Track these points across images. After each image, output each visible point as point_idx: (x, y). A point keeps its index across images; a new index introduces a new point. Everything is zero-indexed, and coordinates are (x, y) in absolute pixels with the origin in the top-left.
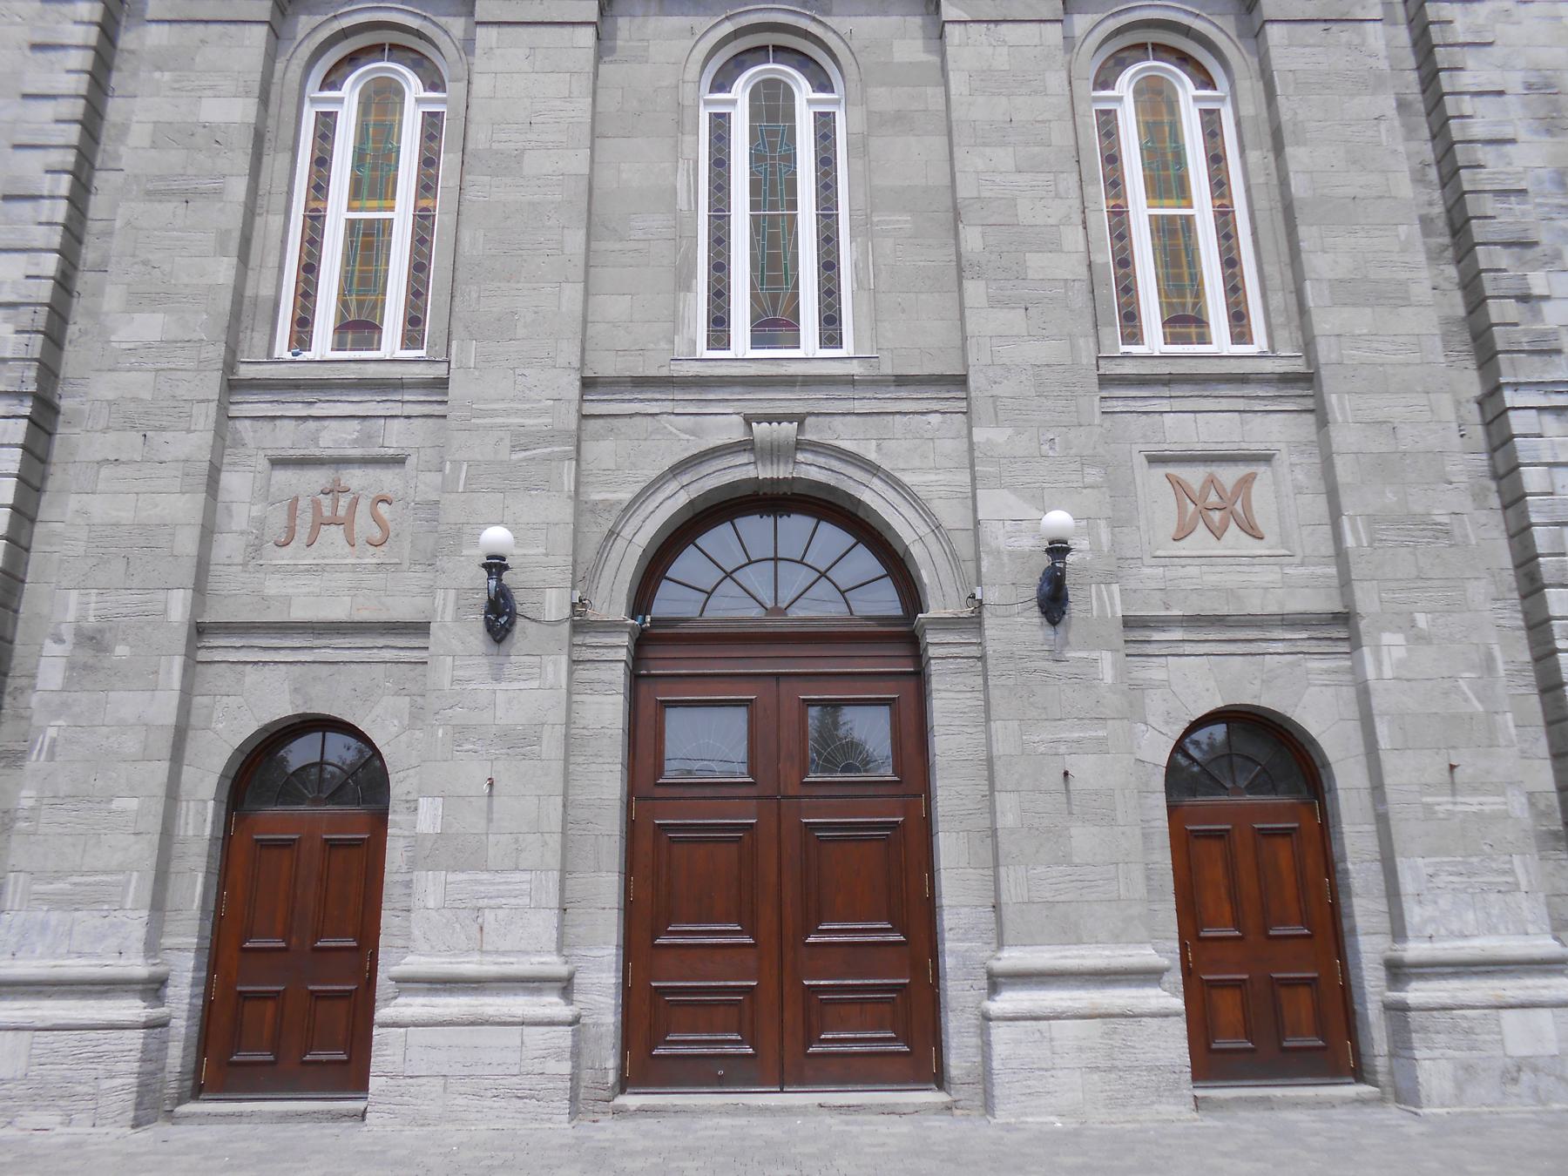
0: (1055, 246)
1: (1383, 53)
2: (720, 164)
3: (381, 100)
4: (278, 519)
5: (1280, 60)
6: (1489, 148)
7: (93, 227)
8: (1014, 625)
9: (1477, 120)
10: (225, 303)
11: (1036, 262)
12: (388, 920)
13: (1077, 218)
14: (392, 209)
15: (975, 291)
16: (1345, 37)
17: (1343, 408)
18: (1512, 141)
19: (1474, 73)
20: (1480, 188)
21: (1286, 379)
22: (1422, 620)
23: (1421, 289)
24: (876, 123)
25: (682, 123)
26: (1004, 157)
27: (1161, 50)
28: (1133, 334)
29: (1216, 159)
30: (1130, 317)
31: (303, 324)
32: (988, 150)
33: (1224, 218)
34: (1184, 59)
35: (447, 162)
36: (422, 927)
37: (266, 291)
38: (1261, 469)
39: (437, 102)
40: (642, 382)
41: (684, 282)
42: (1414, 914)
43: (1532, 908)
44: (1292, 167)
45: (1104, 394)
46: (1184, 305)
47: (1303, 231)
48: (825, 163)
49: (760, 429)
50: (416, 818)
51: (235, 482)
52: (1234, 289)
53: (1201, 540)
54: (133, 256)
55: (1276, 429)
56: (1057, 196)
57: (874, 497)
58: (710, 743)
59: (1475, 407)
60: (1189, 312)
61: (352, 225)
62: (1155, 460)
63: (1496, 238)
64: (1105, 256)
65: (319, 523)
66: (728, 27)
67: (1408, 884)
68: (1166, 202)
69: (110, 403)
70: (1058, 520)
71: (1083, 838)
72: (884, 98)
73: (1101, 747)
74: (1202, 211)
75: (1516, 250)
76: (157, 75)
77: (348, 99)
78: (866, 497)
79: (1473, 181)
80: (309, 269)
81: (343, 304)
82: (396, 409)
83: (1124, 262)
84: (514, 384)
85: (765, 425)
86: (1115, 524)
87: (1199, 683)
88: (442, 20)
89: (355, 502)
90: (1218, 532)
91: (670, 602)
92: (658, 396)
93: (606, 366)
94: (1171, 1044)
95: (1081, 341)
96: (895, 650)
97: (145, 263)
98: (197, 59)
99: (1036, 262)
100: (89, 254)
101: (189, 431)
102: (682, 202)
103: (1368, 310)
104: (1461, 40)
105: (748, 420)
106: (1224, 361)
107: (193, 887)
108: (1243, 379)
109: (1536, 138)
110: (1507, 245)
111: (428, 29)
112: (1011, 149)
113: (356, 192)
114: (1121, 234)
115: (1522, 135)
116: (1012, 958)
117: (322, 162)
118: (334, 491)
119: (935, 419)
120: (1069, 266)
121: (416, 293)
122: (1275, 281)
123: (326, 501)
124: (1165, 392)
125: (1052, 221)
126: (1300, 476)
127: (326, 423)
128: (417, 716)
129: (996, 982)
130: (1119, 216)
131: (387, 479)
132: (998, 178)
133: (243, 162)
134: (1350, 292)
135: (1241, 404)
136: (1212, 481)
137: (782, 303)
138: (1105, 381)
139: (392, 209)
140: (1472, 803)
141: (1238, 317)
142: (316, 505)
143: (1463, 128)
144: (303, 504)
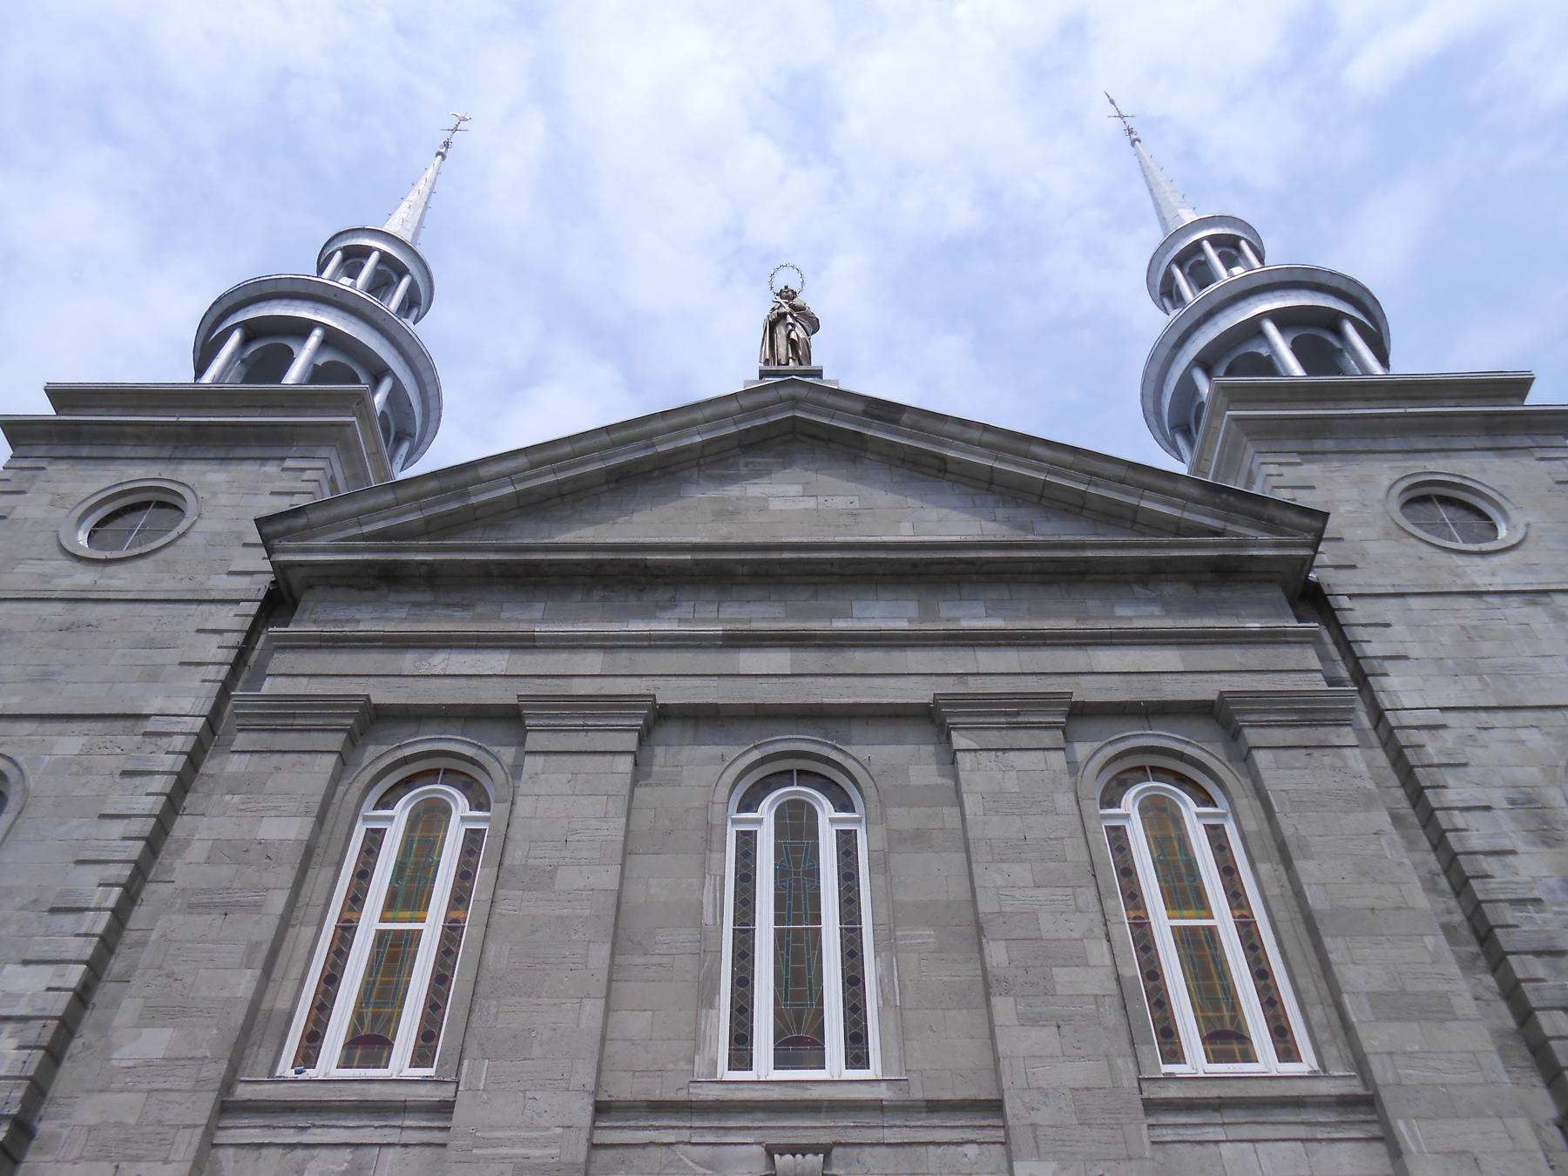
0: (1081, 961)
1: (1366, 774)
2: (746, 878)
3: (430, 819)
6: (1490, 859)
7: (129, 937)
9: (1475, 834)
10: (238, 1018)
11: (1062, 975)
13: (1099, 931)
14: (423, 920)
15: (1003, 1007)
16: (1327, 760)
17: (1413, 1135)
18: (1513, 852)
19: (1455, 792)
20: (1493, 897)
21: (1345, 1103)
23: (1463, 1001)
24: (897, 841)
25: (710, 840)
26: (1021, 873)
27: (1159, 773)
28: (1174, 1053)
29: (1228, 871)
30: (1168, 1033)
31: (313, 1037)
32: (1006, 866)
34: (1182, 780)
40: (659, 1108)
41: (707, 998)
44: (1304, 879)
45: (1152, 1121)
46: (1221, 1019)
47: (1328, 942)
48: (848, 878)
52: (1270, 1001)
54: (159, 968)
56: (1078, 910)
59: (1556, 1131)
60: (1228, 1027)
61: (381, 935)
63: (1524, 947)
64: (1133, 970)
66: (756, 755)
68: (1185, 913)
69: (91, 1128)
72: (902, 818)
74: (1223, 922)
75: (1548, 959)
76: (228, 797)
79: (1486, 891)
80: (331, 980)
81: (358, 1016)
82: (393, 1136)
83: (1153, 974)
85: (788, 1157)
88: (495, 749)
92: (674, 1123)
93: (623, 1089)
95: (1120, 1062)
98: (269, 783)
99: (1062, 975)
100: (116, 965)
101: (166, 1161)
102: (708, 918)
103: (1415, 1025)
104: (1436, 761)
105: (771, 1151)
106: (1275, 1083)
108: (1298, 1103)
109: (1534, 849)
110: (1538, 953)
111: (481, 756)
112: (1028, 865)
113: (391, 903)
114: (1146, 946)
115: (1520, 846)
117: (363, 875)
119: (972, 1150)
120: (1093, 979)
121: (434, 1007)
122: (1312, 994)
124: (1217, 1118)
125: (1075, 935)
127: (315, 1152)
130: (1142, 929)
132: (1018, 893)
133: (288, 876)
134: (1394, 1004)
135: (1302, 1132)
137: (807, 1019)
138: (1151, 1106)
139: (423, 920)
141: (1280, 1032)
143: (1460, 840)
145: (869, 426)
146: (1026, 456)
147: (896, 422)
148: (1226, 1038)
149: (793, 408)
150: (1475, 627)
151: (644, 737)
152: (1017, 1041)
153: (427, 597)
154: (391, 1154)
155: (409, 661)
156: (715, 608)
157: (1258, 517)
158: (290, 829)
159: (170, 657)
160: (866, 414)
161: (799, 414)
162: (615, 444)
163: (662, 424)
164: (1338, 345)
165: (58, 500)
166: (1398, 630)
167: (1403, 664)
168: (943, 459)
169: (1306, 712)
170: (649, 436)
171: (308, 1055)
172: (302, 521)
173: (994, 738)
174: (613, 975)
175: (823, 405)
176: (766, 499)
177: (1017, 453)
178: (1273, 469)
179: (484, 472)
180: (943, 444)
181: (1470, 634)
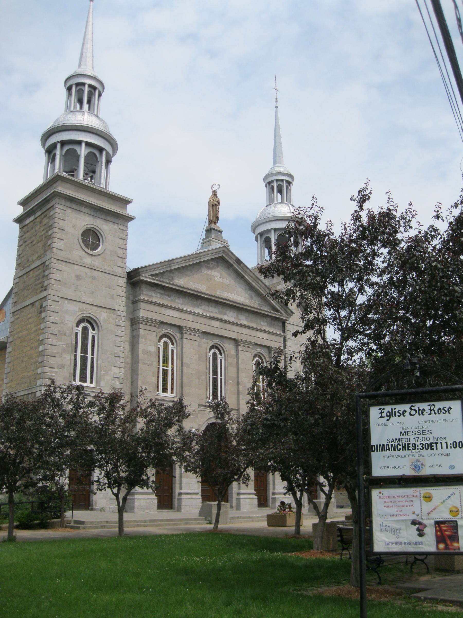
42: (276, 487)
88: (176, 334)
94: (256, 502)
97: (143, 376)
145: (235, 263)
146: (258, 283)
147: (240, 265)
149: (223, 253)
153: (162, 292)
155: (163, 310)
156: (207, 307)
157: (285, 310)
160: (235, 261)
161: (224, 256)
162: (195, 258)
163: (203, 254)
168: (244, 277)
170: (200, 257)
172: (146, 269)
175: (229, 255)
176: (214, 277)
177: (256, 282)
179: (175, 261)
180: (245, 274)
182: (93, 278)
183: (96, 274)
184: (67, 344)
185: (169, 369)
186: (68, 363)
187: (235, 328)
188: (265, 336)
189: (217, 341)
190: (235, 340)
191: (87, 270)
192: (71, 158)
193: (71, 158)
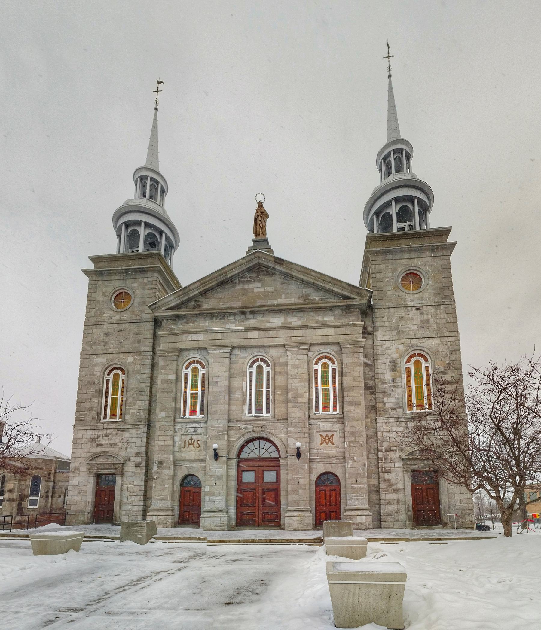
4: (183, 444)
5: (345, 361)
8: (293, 460)
11: (300, 399)
12: (202, 503)
15: (290, 405)
16: (356, 356)
22: (355, 458)
24: (275, 374)
25: (244, 375)
26: (296, 380)
29: (334, 378)
31: (185, 411)
33: (334, 389)
35: (206, 382)
36: (207, 503)
37: (178, 407)
38: (335, 433)
39: (204, 371)
41: (244, 403)
42: (348, 502)
43: (366, 501)
44: (344, 381)
47: (344, 393)
49: (255, 429)
50: (206, 489)
51: (177, 438)
53: (324, 445)
55: (338, 426)
57: (273, 439)
58: (249, 477)
61: (191, 393)
62: (317, 432)
65: (189, 444)
66: (252, 356)
67: (348, 498)
70: (298, 444)
71: (300, 491)
72: (278, 369)
73: (304, 478)
77: (189, 372)
78: (272, 439)
80: (185, 402)
81: (191, 407)
84: (218, 423)
86: (310, 443)
87: (320, 468)
89: (194, 441)
90: (327, 444)
91: (243, 455)
96: (274, 463)
99: (300, 399)
102: (244, 390)
107: (177, 497)
113: (192, 388)
116: (289, 508)
117: (186, 383)
118: (191, 439)
119: (283, 426)
121: (202, 406)
123: (190, 441)
126: (341, 435)
128: (205, 474)
129: (287, 511)
131: (199, 437)
134: (351, 404)
136: (327, 435)
140: (359, 486)
141: (335, 407)
142: (189, 442)
144: (187, 442)
148: (326, 408)
150: (402, 317)
151: (231, 351)
152: (291, 410)
154: (200, 429)
158: (172, 377)
159: (141, 337)
164: (411, 209)
165: (104, 294)
166: (385, 319)
167: (382, 328)
169: (355, 346)
171: (185, 414)
173: (295, 352)
174: (230, 400)
178: (373, 267)
181: (401, 318)
182: (121, 330)
183: (123, 326)
184: (96, 390)
185: (199, 392)
186: (96, 405)
187: (282, 333)
188: (331, 331)
189: (260, 352)
190: (284, 346)
191: (115, 326)
192: (133, 237)
193: (133, 237)
